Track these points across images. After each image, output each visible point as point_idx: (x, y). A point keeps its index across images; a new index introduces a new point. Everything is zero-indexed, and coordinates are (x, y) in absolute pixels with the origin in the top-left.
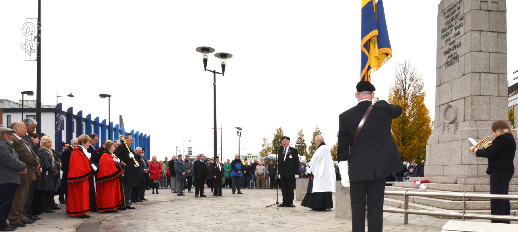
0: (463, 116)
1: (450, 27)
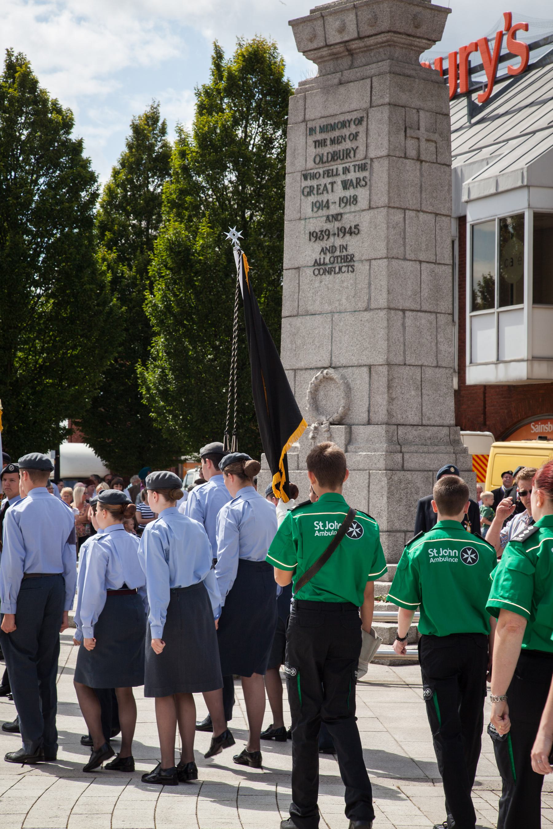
0: (365, 408)
1: (329, 173)
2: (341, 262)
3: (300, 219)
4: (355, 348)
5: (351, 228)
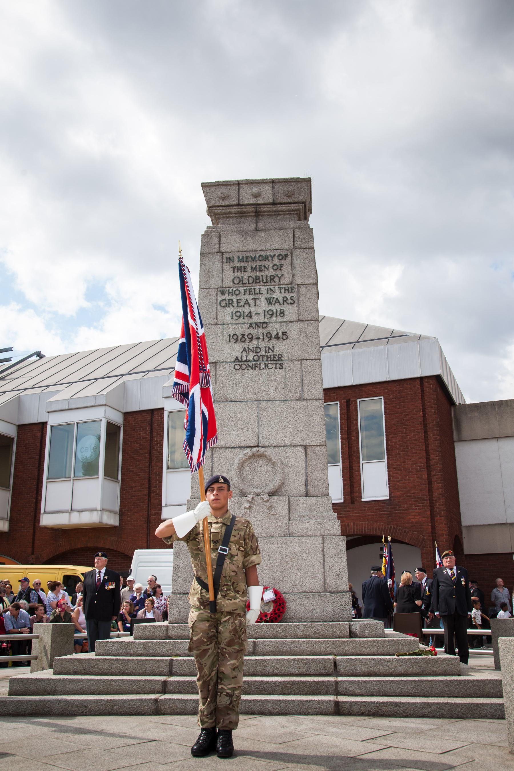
2: (267, 361)
3: (217, 324)
5: (277, 334)
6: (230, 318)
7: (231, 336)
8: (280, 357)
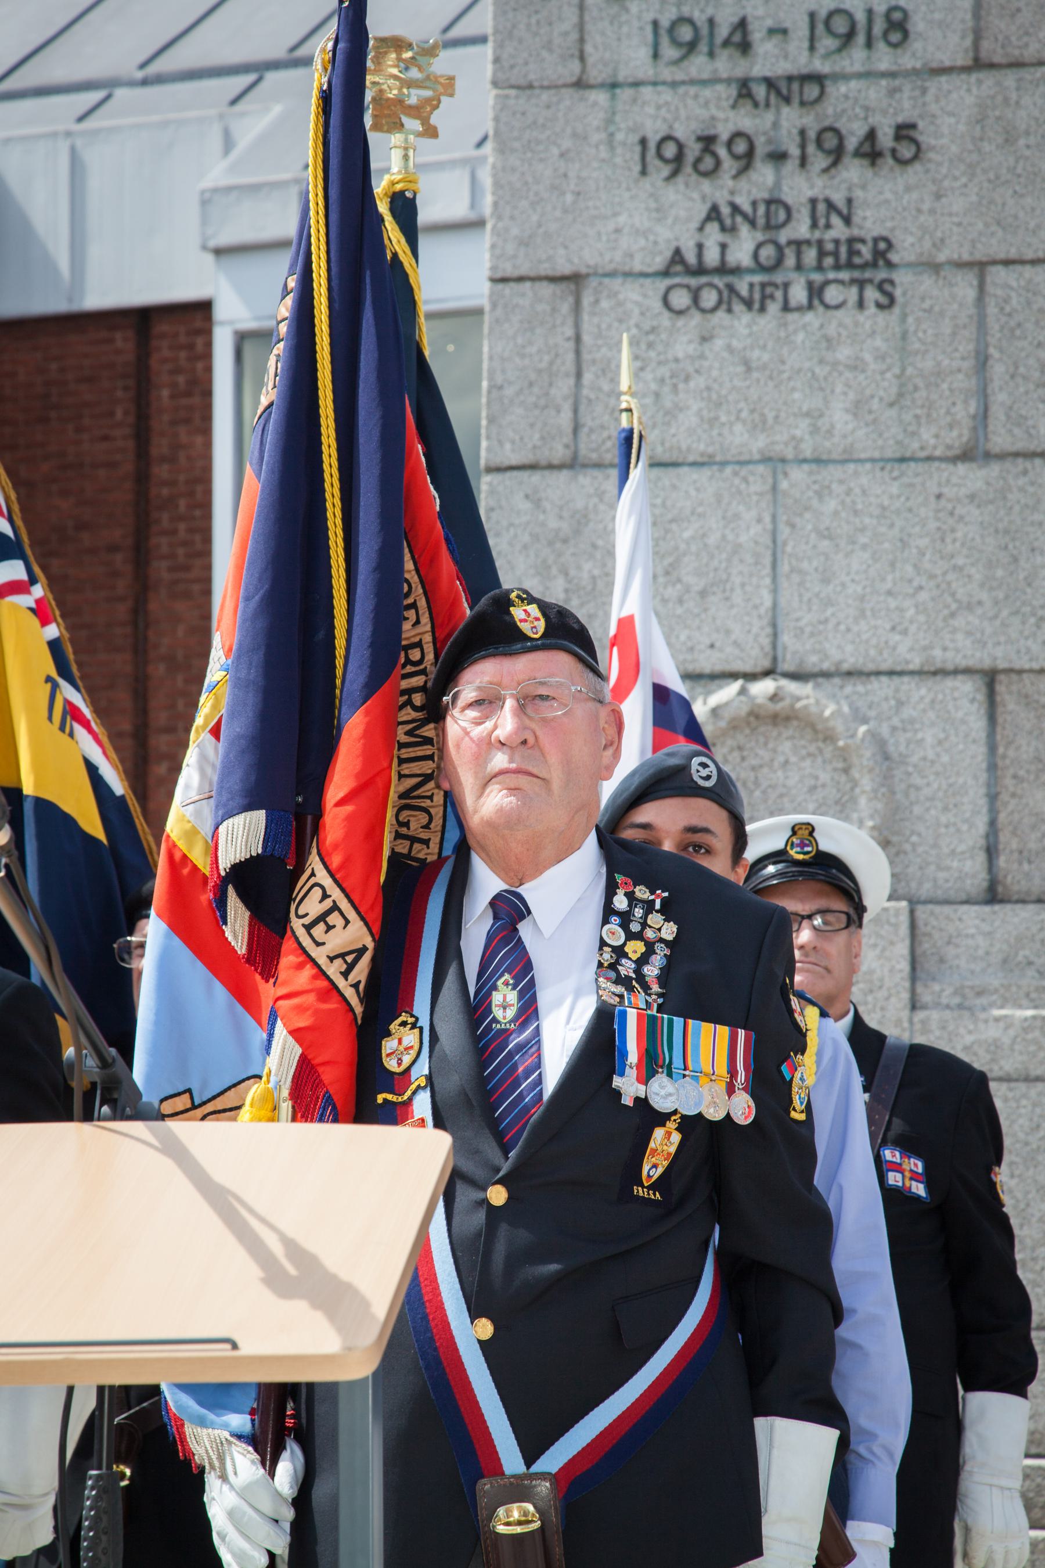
2: (820, 268)
3: (580, 84)
4: (908, 603)
5: (871, 135)
6: (644, 53)
7: (652, 146)
8: (882, 252)
